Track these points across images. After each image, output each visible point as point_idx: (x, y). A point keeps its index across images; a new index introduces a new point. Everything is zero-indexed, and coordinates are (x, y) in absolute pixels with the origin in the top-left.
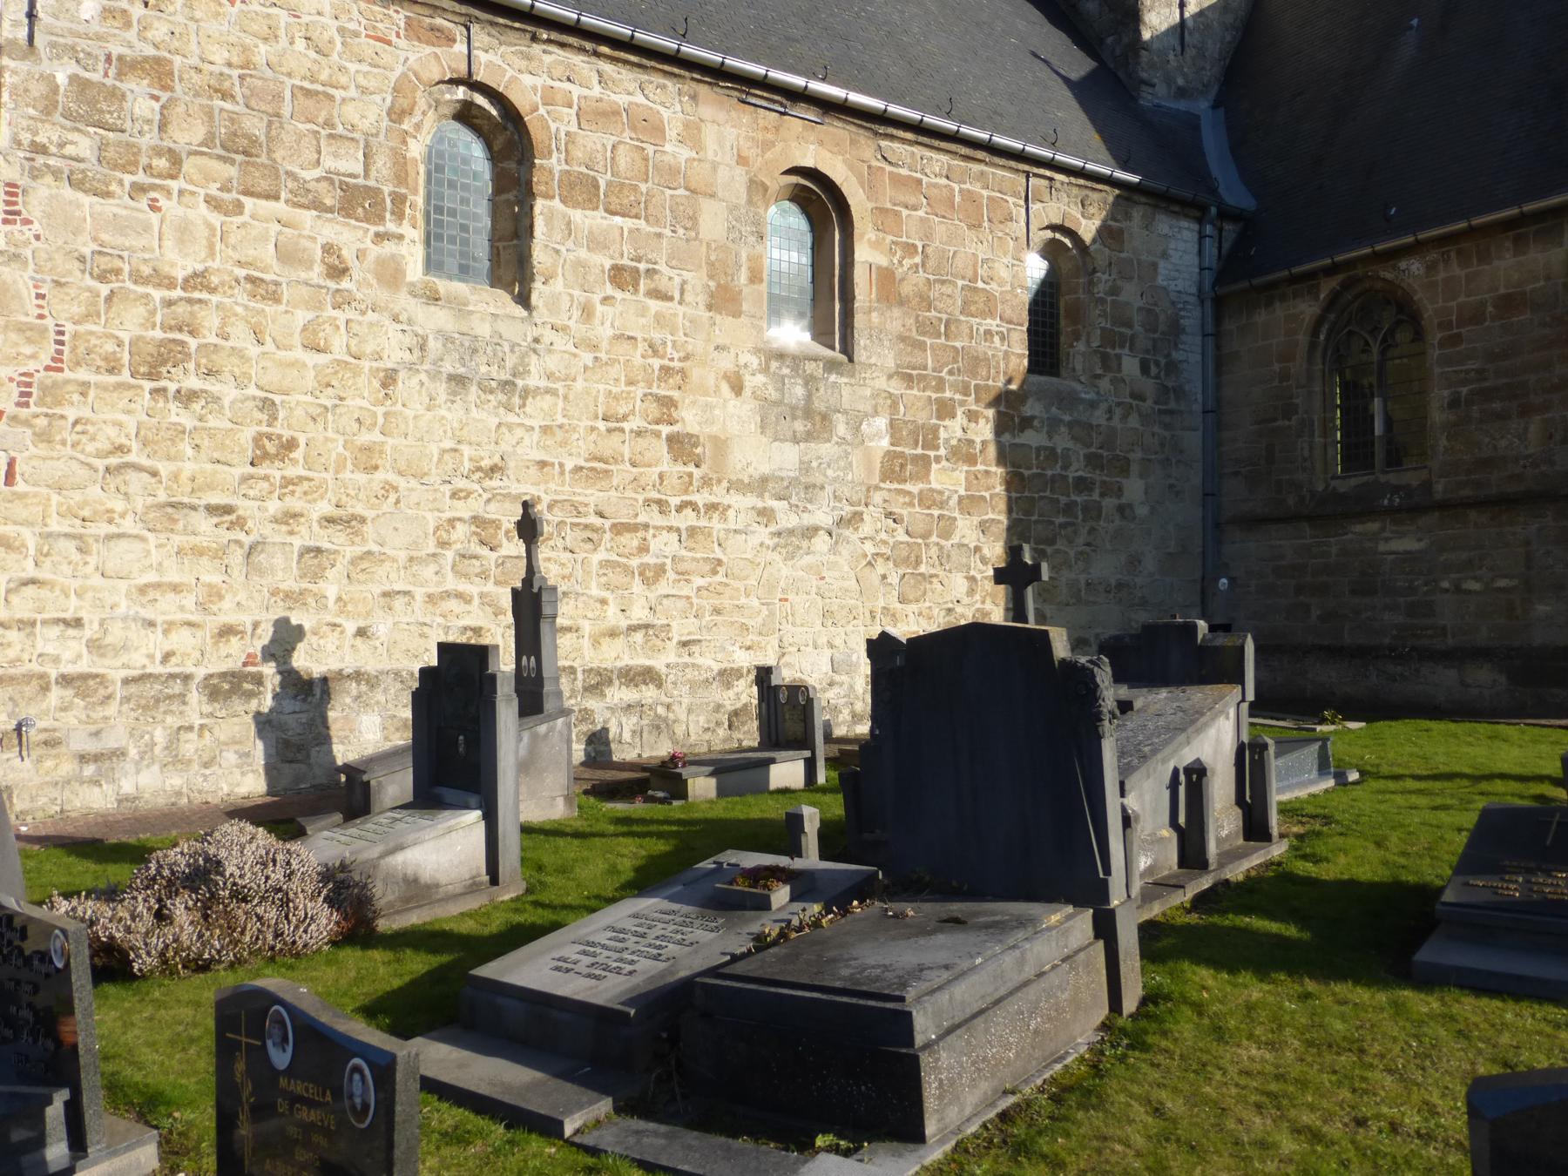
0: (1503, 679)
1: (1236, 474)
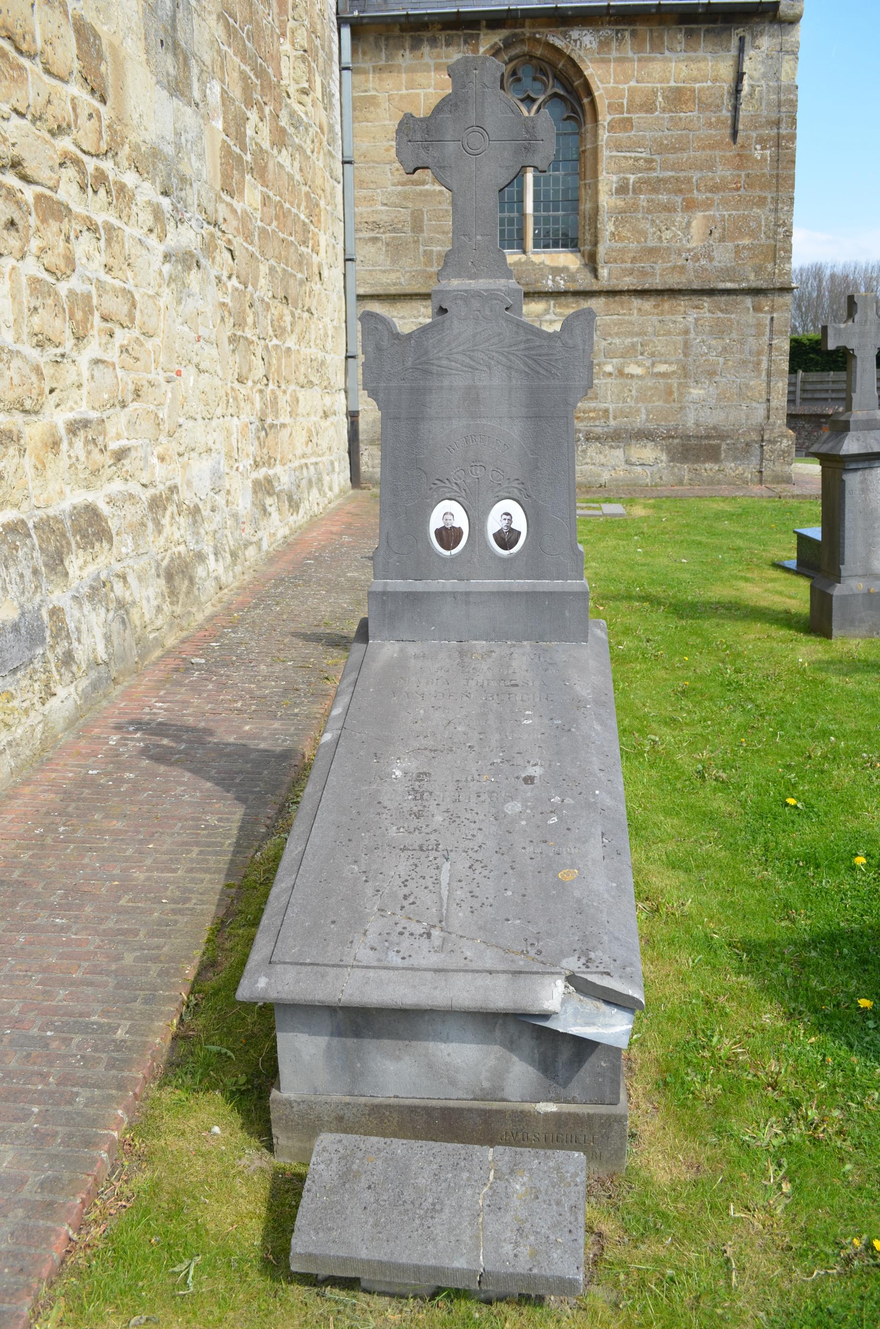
0: (664, 457)
1: (375, 240)
